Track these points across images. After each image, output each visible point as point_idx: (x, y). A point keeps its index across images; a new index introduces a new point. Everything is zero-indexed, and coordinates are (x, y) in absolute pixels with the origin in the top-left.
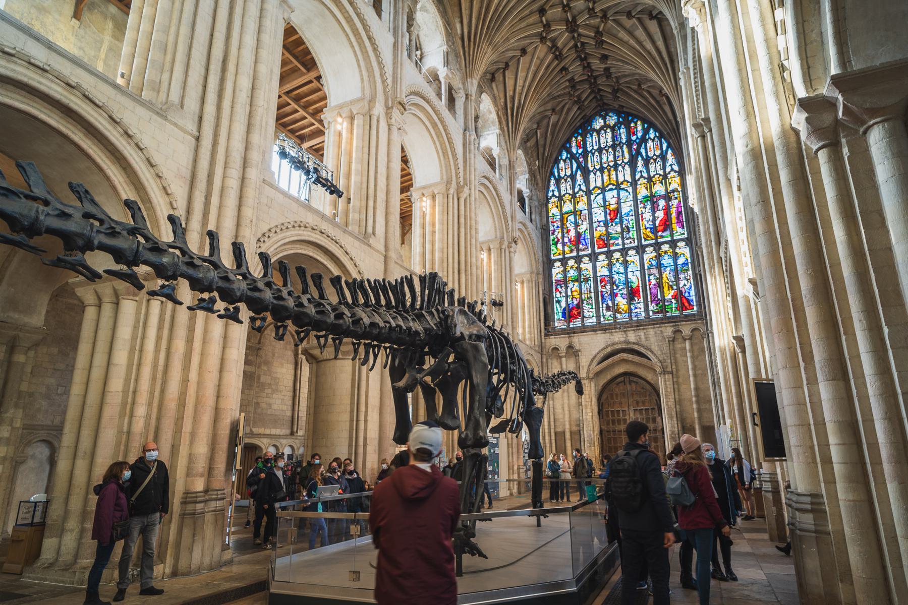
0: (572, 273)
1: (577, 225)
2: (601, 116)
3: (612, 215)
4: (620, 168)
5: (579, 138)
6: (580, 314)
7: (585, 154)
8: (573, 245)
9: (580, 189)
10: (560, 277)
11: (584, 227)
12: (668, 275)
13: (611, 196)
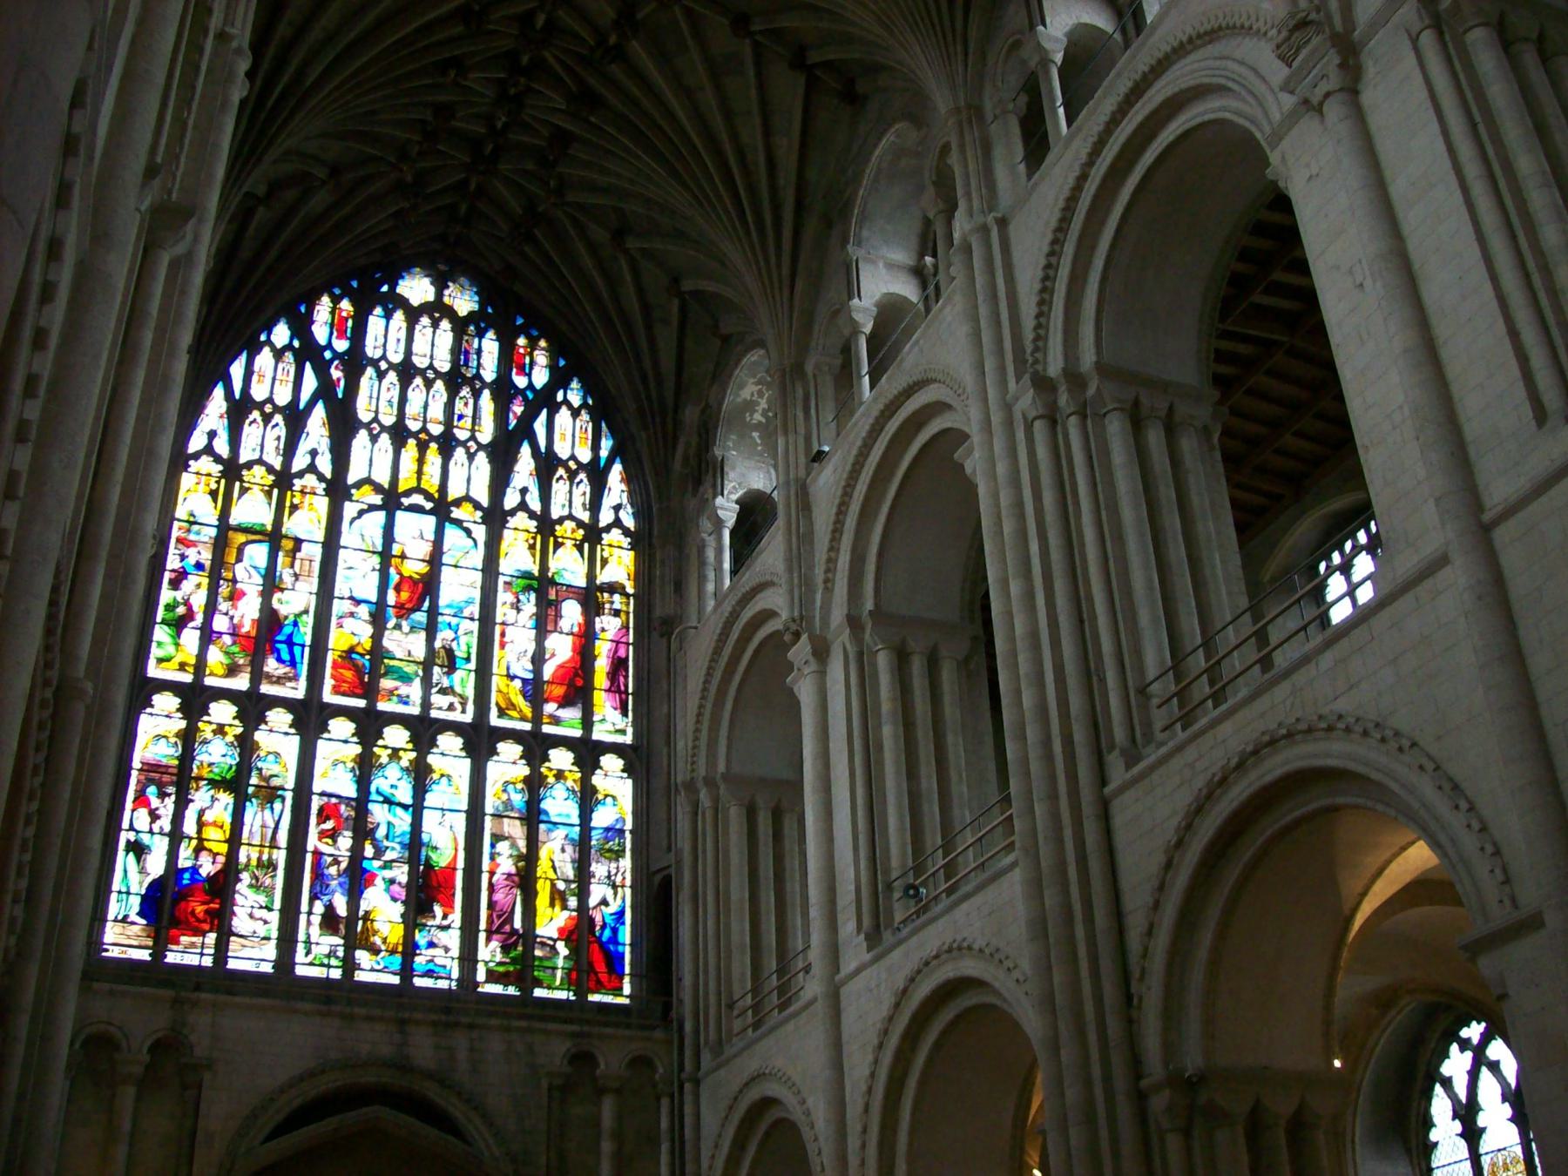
0: (217, 754)
1: (271, 584)
3: (405, 595)
4: (460, 453)
5: (346, 305)
6: (221, 921)
10: (166, 753)
11: (296, 600)
13: (414, 531)
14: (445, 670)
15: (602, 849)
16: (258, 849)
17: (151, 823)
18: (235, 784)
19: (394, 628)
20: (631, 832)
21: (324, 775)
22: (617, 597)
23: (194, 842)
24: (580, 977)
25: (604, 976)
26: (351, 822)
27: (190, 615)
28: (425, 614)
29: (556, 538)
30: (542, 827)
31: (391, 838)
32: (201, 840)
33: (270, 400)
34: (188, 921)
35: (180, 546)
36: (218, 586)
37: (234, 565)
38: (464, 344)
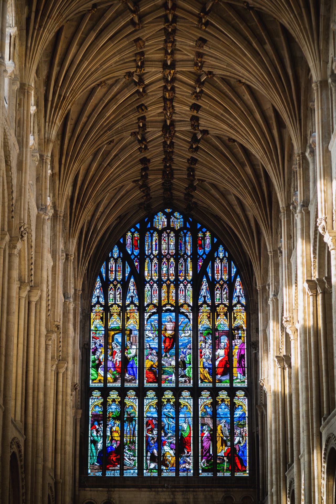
0: (114, 408)
1: (124, 348)
2: (165, 213)
3: (167, 344)
6: (121, 461)
7: (142, 257)
8: (118, 372)
9: (132, 302)
11: (133, 351)
12: (222, 426)
14: (182, 369)
17: (97, 434)
18: (120, 418)
19: (165, 356)
20: (247, 417)
21: (147, 411)
23: (110, 438)
24: (233, 469)
26: (157, 425)
27: (100, 363)
29: (217, 312)
30: (218, 419)
31: (169, 429)
32: (112, 437)
33: (115, 279)
35: (94, 339)
38: (180, 241)
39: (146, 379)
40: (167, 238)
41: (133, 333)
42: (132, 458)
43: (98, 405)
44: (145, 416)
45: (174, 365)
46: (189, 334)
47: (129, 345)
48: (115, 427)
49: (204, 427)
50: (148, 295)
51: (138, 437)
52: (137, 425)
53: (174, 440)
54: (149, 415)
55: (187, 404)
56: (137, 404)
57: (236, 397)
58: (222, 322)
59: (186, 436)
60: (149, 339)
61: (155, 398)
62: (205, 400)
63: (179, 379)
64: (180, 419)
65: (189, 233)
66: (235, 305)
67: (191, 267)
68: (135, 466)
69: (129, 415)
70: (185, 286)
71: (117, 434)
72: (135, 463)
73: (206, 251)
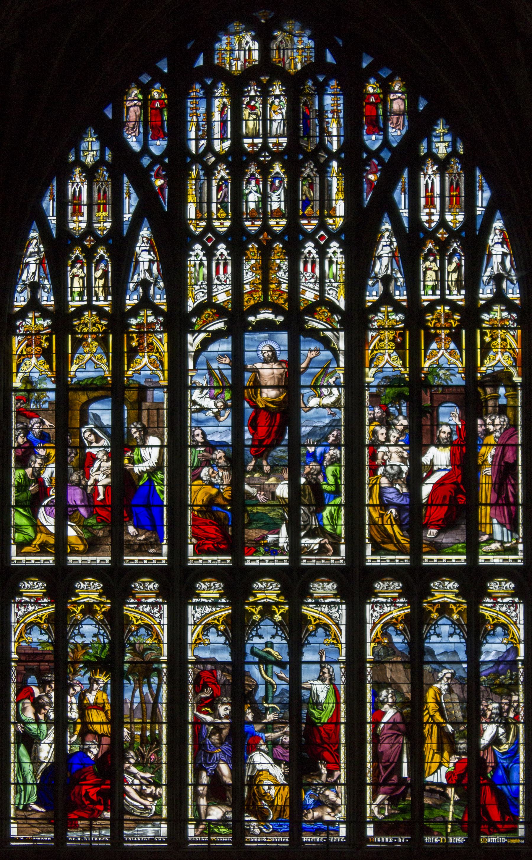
3: (262, 431)
14: (313, 508)
15: (493, 684)
16: (140, 726)
17: (35, 714)
19: (254, 470)
21: (197, 643)
22: (502, 391)
23: (79, 727)
25: (495, 814)
27: (43, 492)
28: (286, 449)
29: (427, 329)
30: (427, 667)
31: (270, 699)
34: (83, 803)
36: (66, 455)
37: (79, 429)
39: (194, 540)
40: (259, 100)
41: (149, 397)
42: (148, 791)
43: (38, 624)
44: (190, 657)
45: (286, 496)
46: (333, 399)
47: (137, 435)
48: (94, 693)
49: (384, 693)
50: (197, 279)
51: (169, 723)
52: (164, 687)
53: (285, 733)
54: (204, 654)
55: (329, 622)
56: (165, 621)
57: (488, 600)
58: (442, 361)
59: (325, 720)
60: (201, 416)
61: (223, 600)
62: (386, 609)
63: (303, 541)
64: (303, 665)
65: (333, 83)
66: (488, 307)
67: (341, 188)
68: (161, 815)
69: (141, 654)
70: (322, 251)
71: (102, 714)
72: (160, 806)
73: (391, 138)
